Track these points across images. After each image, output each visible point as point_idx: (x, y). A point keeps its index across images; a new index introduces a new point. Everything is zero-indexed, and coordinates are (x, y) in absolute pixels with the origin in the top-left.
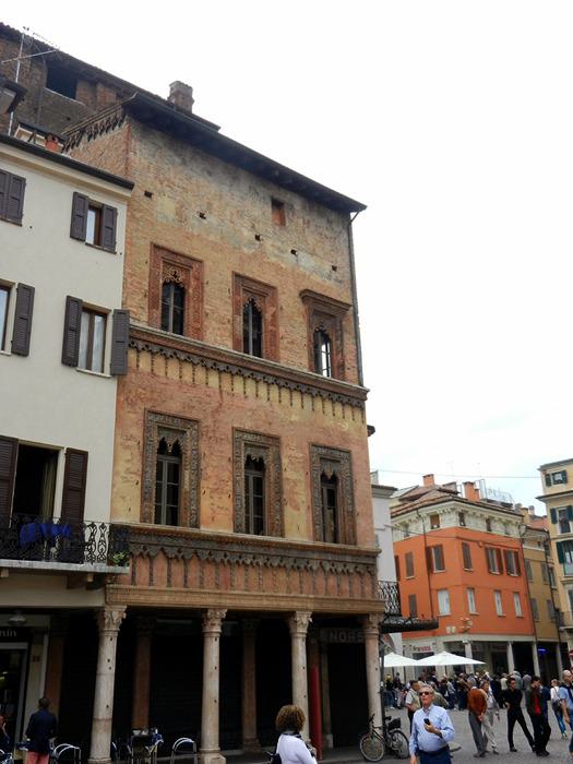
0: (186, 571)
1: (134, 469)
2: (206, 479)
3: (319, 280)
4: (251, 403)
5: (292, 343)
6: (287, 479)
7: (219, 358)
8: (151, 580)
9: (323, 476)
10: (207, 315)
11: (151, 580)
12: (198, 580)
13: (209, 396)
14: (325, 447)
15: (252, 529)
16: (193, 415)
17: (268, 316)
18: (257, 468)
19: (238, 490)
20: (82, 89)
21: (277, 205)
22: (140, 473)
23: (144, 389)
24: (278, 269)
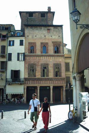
4: (44, 60)
16: (35, 63)
18: (45, 68)
20: (34, 15)
21: (48, 30)
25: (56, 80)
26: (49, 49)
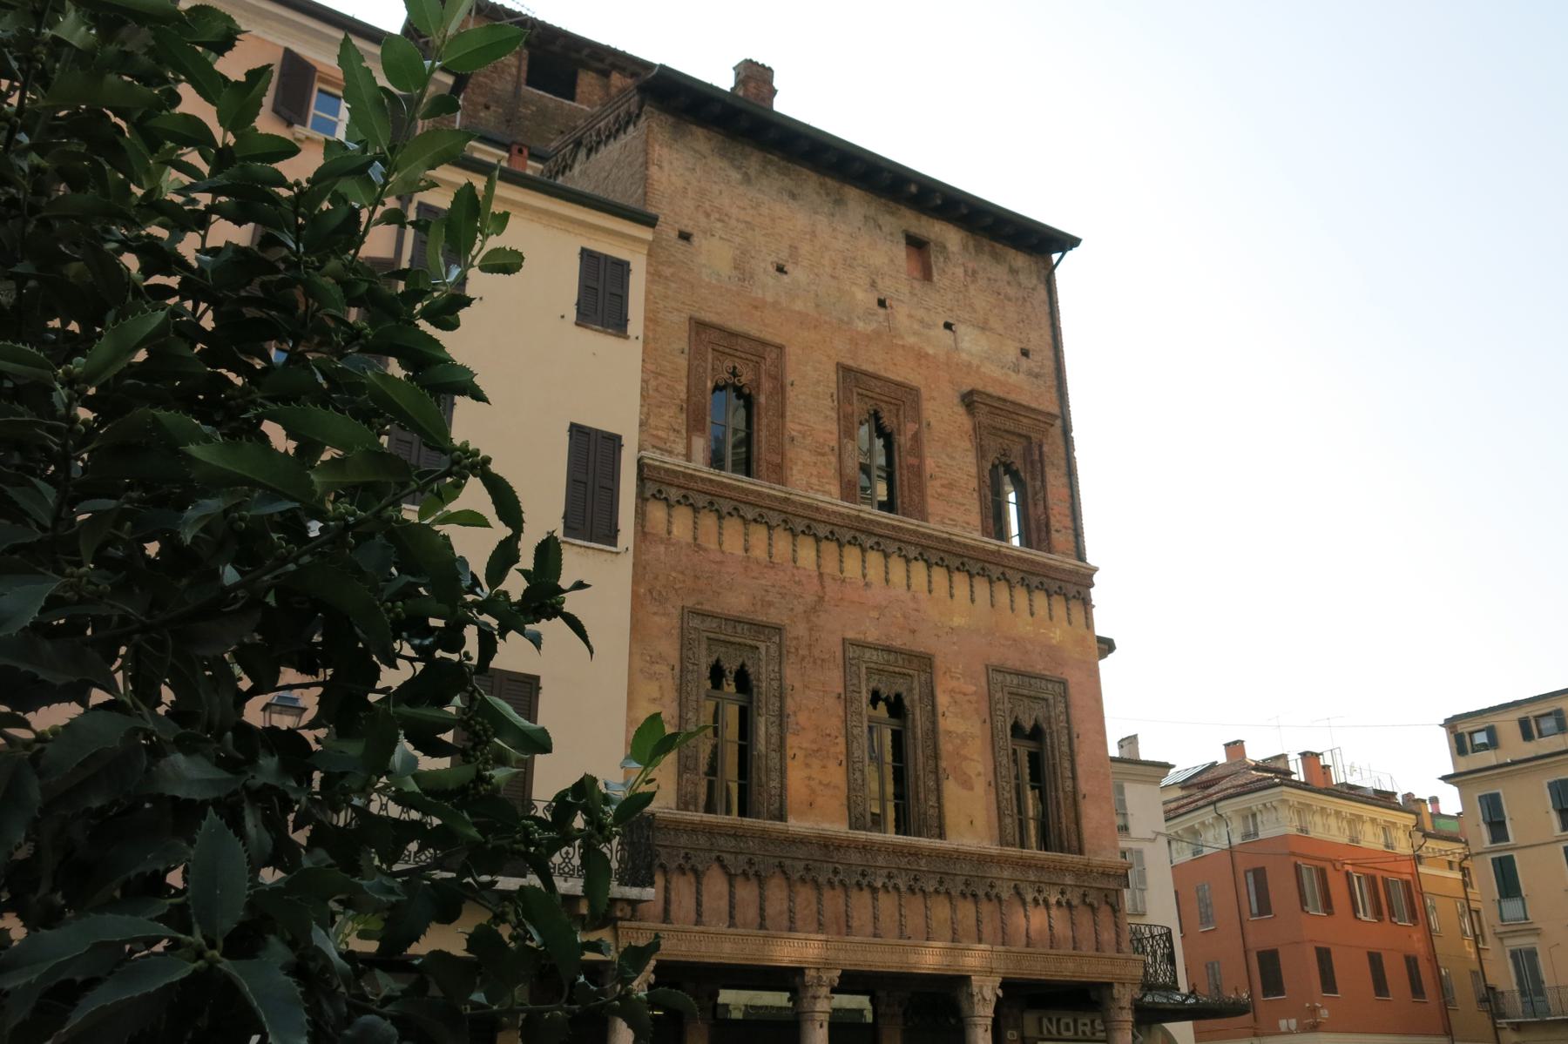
0: (762, 898)
3: (997, 373)
8: (699, 914)
9: (1016, 729)
10: (793, 439)
11: (699, 914)
12: (786, 916)
13: (799, 583)
14: (1018, 673)
16: (773, 616)
17: (903, 440)
20: (587, 82)
21: (917, 244)
24: (921, 356)
26: (930, 464)
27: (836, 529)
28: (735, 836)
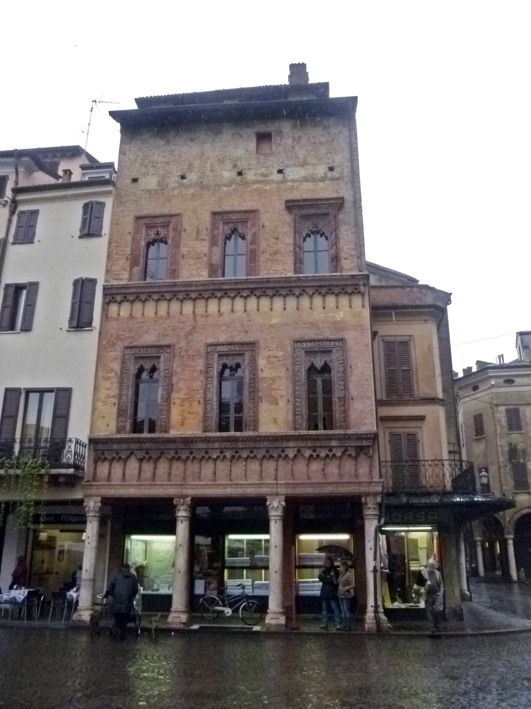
0: (155, 469)
1: (113, 394)
2: (177, 392)
4: (227, 318)
5: (275, 253)
6: (265, 378)
7: (189, 288)
9: (312, 369)
12: (167, 475)
13: (183, 322)
14: (311, 341)
15: (321, 425)
16: (168, 341)
19: (209, 396)
21: (263, 138)
22: (117, 396)
23: (124, 331)
25: (307, 453)
27: (202, 292)
28: (138, 442)
